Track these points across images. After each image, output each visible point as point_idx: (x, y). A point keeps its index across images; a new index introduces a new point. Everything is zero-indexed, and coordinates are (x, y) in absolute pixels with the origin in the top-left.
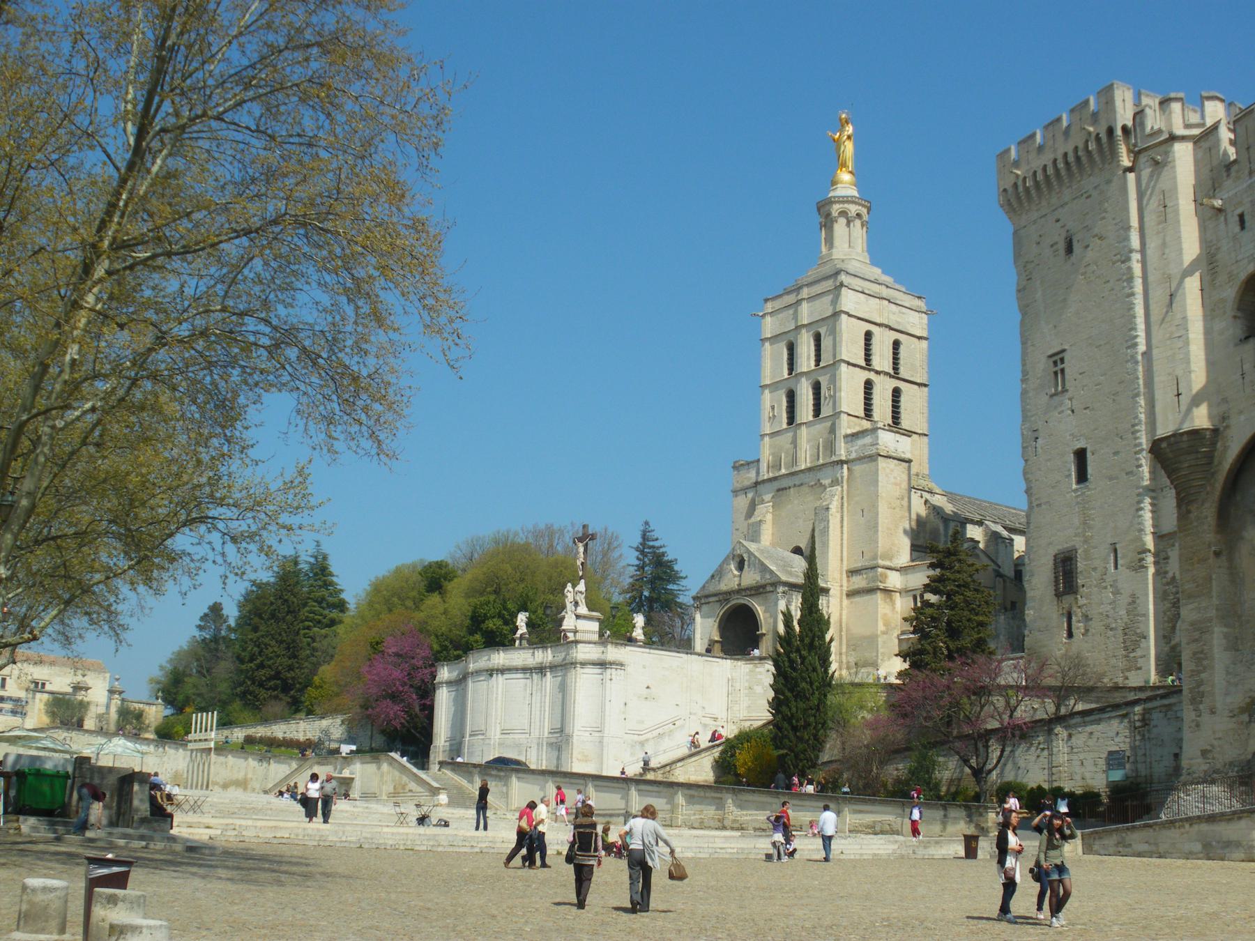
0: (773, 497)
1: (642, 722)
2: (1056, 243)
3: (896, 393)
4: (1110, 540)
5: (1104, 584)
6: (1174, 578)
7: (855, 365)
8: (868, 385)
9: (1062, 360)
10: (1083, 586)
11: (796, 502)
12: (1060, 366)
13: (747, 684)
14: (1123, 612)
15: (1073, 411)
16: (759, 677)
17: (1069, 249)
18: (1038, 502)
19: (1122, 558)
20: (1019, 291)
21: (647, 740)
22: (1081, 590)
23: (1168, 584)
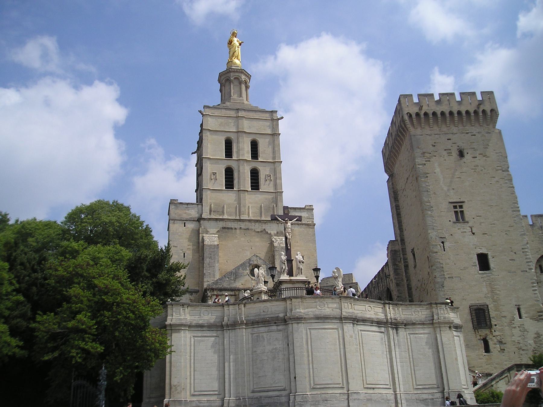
0: (218, 231)
5: (514, 326)
9: (461, 207)
10: (496, 325)
11: (243, 239)
12: (458, 209)
14: (531, 342)
15: (474, 234)
17: (461, 154)
18: (449, 276)
19: (525, 313)
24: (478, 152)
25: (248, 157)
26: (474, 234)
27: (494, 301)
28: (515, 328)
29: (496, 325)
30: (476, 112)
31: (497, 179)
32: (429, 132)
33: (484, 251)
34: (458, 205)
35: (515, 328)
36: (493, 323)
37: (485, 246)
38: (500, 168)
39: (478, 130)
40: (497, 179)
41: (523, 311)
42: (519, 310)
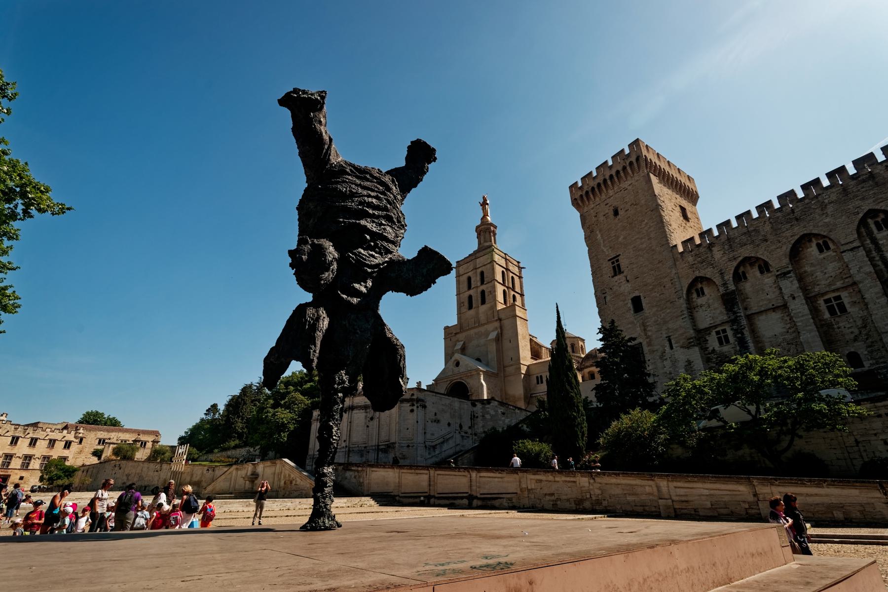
1: (433, 434)
2: (608, 213)
3: (514, 297)
4: (665, 336)
5: (665, 358)
6: (714, 351)
7: (499, 283)
8: (504, 291)
9: (617, 261)
10: (649, 360)
12: (616, 264)
13: (481, 414)
15: (628, 281)
16: (488, 410)
17: (616, 213)
20: (585, 238)
21: (436, 445)
22: (647, 362)
23: (709, 354)
24: (629, 204)
25: (479, 284)
26: (628, 281)
27: (648, 337)
28: (666, 359)
29: (649, 360)
30: (624, 168)
31: (646, 221)
32: (593, 206)
33: (637, 294)
34: (614, 260)
35: (666, 359)
36: (647, 359)
37: (637, 290)
38: (648, 210)
39: (629, 183)
40: (646, 221)
41: (673, 342)
42: (670, 341)
